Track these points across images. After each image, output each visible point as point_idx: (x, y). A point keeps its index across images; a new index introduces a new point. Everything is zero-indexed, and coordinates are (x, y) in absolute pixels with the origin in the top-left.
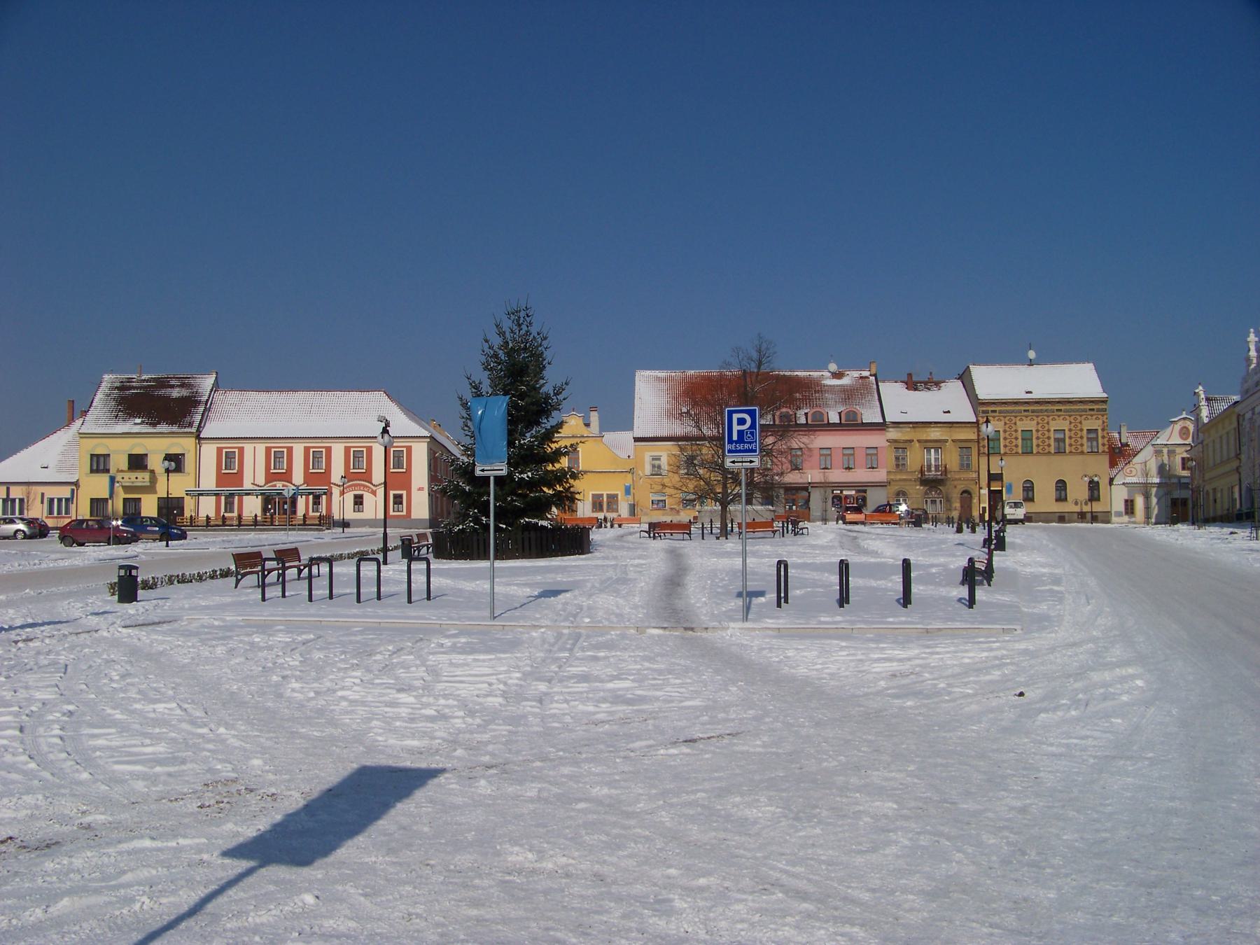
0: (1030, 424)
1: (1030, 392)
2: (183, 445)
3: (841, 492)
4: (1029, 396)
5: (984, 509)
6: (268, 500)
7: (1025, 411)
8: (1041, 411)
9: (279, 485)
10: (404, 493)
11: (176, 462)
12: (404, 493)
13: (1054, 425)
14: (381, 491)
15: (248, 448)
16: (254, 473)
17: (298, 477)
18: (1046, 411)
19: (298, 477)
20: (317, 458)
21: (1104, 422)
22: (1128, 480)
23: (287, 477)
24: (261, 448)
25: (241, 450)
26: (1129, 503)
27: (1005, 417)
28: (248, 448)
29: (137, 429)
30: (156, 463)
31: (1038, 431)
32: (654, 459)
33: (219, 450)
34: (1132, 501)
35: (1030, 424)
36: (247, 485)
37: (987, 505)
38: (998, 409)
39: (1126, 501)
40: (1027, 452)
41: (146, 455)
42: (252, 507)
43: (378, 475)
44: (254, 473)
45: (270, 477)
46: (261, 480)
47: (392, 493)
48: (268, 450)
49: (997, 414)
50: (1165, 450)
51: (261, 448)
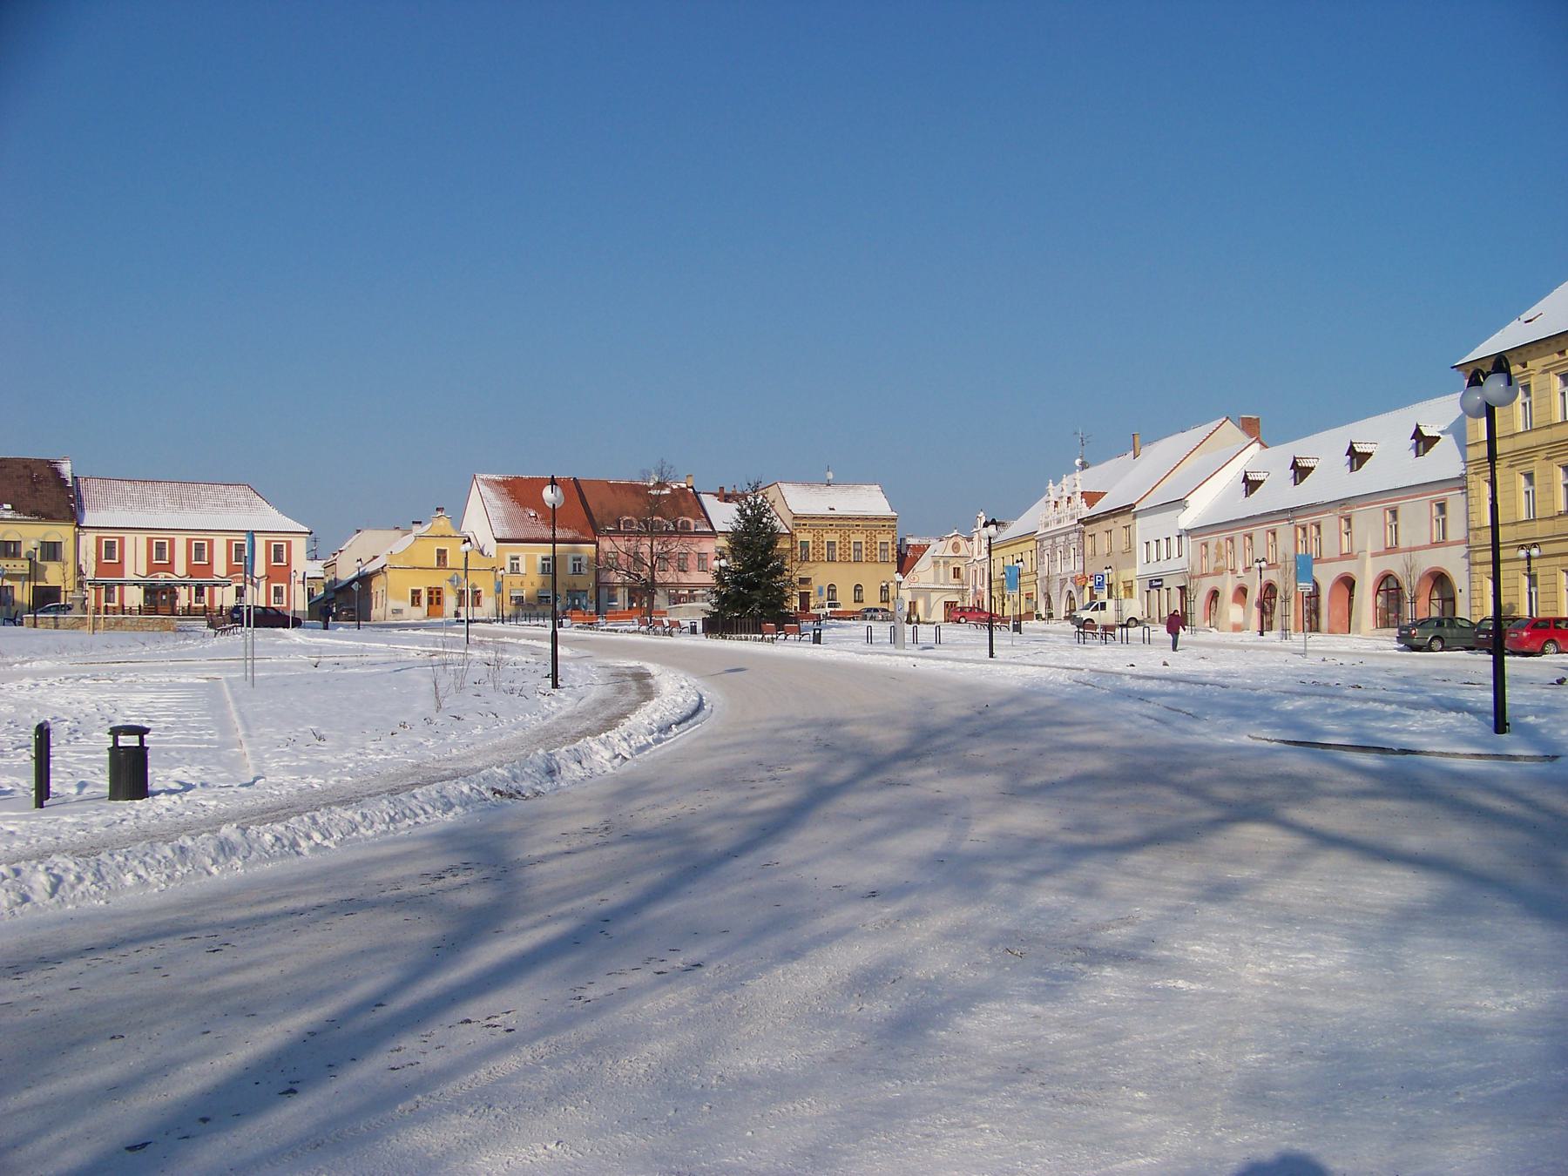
0: (861, 538)
1: (833, 509)
2: (60, 532)
3: (677, 591)
4: (832, 512)
5: (796, 608)
6: (151, 591)
7: (830, 525)
8: (844, 525)
9: (161, 576)
10: (285, 585)
11: (51, 551)
13: (854, 538)
14: (263, 584)
15: (129, 538)
16: (135, 563)
17: (181, 568)
18: (848, 525)
19: (181, 568)
20: (199, 549)
21: (893, 537)
22: (913, 585)
23: (170, 567)
24: (142, 538)
25: (122, 540)
26: (912, 604)
27: (867, 531)
28: (129, 538)
29: (8, 515)
31: (867, 543)
32: (513, 558)
33: (99, 540)
34: (915, 603)
35: (861, 538)
36: (129, 575)
37: (798, 605)
38: (808, 522)
39: (910, 603)
40: (831, 560)
41: (61, 543)
42: (135, 597)
43: (260, 569)
44: (135, 563)
45: (152, 569)
46: (143, 570)
47: (273, 585)
48: (150, 541)
49: (861, 528)
50: (941, 561)
51: (142, 538)
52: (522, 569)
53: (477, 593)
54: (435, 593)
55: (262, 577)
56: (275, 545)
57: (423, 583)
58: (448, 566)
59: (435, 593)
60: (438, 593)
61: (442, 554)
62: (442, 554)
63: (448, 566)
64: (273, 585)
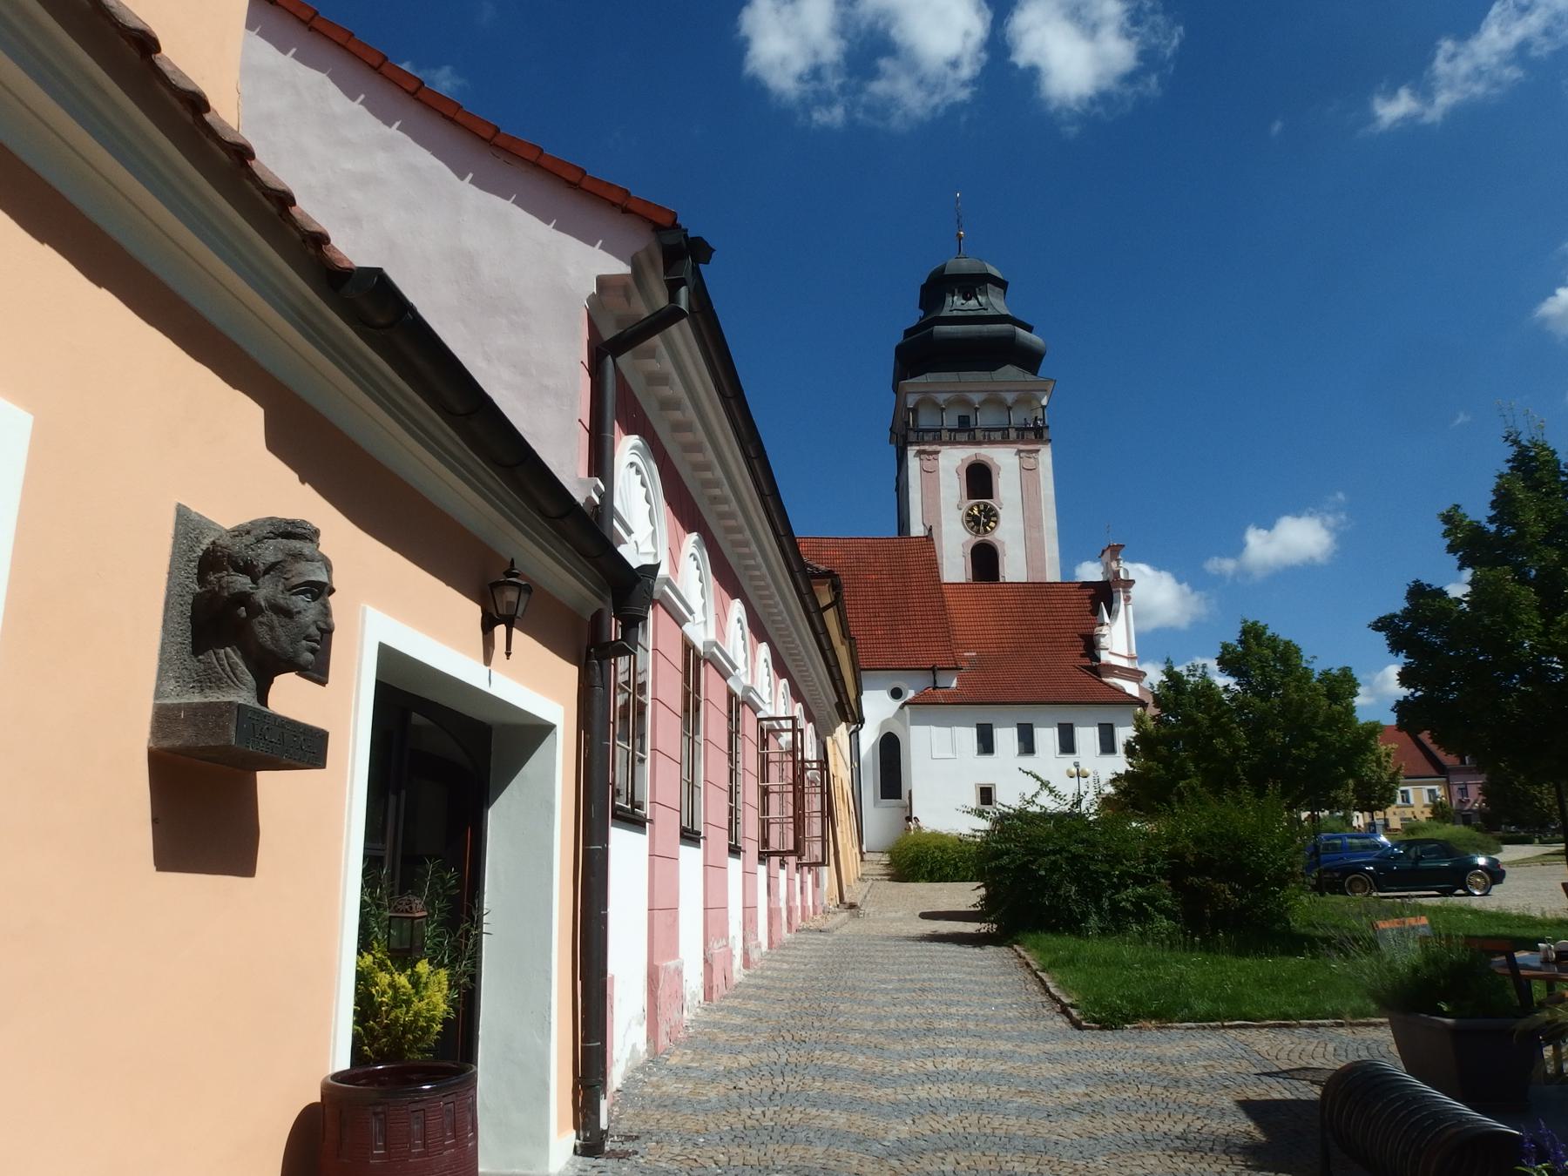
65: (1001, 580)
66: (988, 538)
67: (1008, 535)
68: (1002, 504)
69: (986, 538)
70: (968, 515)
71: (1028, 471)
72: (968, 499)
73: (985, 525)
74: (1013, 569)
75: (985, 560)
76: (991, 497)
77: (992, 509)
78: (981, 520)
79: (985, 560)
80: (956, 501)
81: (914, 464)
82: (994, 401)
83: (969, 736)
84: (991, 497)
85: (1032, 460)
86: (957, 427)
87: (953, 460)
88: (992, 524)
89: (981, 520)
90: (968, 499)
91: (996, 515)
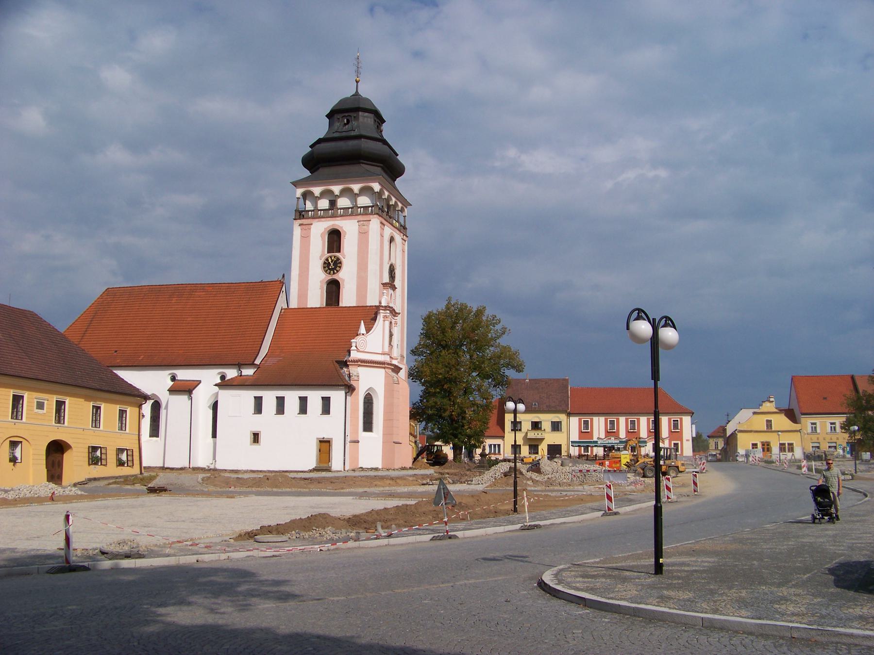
10: (679, 442)
12: (679, 442)
17: (623, 435)
30: (546, 426)
46: (603, 436)
47: (673, 442)
52: (818, 431)
53: (791, 445)
54: (766, 445)
55: (667, 438)
56: (630, 421)
57: (758, 439)
58: (773, 429)
59: (766, 445)
60: (768, 445)
61: (769, 423)
62: (769, 423)
63: (773, 429)
64: (673, 442)
65: (341, 305)
66: (335, 277)
67: (347, 275)
68: (345, 256)
69: (333, 277)
70: (325, 263)
71: (363, 235)
72: (328, 253)
73: (335, 268)
74: (348, 298)
75: (333, 289)
76: (339, 251)
77: (338, 259)
78: (332, 265)
79: (333, 289)
80: (319, 254)
81: (297, 231)
82: (346, 192)
83: (252, 403)
84: (339, 251)
85: (366, 227)
86: (328, 208)
87: (319, 229)
88: (338, 268)
89: (332, 265)
90: (328, 253)
91: (340, 263)
